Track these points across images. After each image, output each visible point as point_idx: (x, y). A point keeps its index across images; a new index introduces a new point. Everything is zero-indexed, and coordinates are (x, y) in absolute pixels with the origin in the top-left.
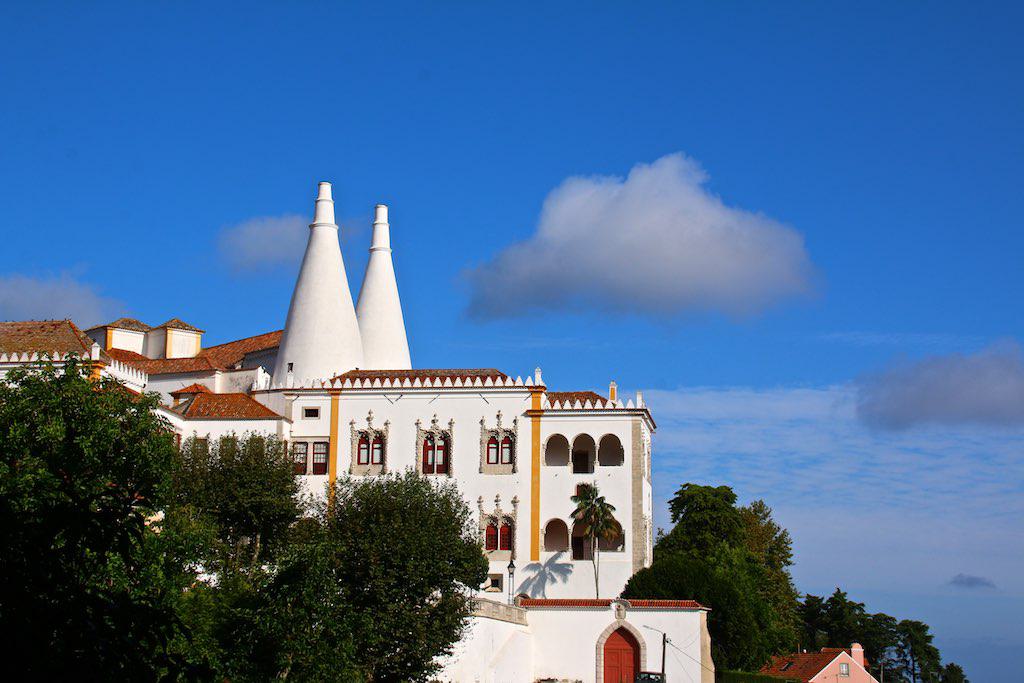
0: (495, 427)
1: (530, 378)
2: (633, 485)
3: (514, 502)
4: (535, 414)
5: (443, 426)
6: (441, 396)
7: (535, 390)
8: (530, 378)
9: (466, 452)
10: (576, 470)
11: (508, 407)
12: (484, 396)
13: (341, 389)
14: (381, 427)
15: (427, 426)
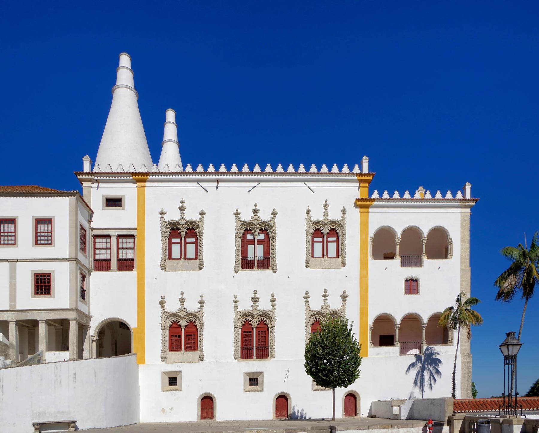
0: (321, 218)
1: (357, 165)
2: (462, 278)
3: (344, 297)
4: (363, 204)
5: (265, 216)
6: (262, 184)
7: (361, 179)
8: (357, 165)
9: (290, 242)
10: (404, 264)
11: (335, 194)
12: (309, 184)
13: (147, 174)
14: (196, 218)
15: (247, 216)
